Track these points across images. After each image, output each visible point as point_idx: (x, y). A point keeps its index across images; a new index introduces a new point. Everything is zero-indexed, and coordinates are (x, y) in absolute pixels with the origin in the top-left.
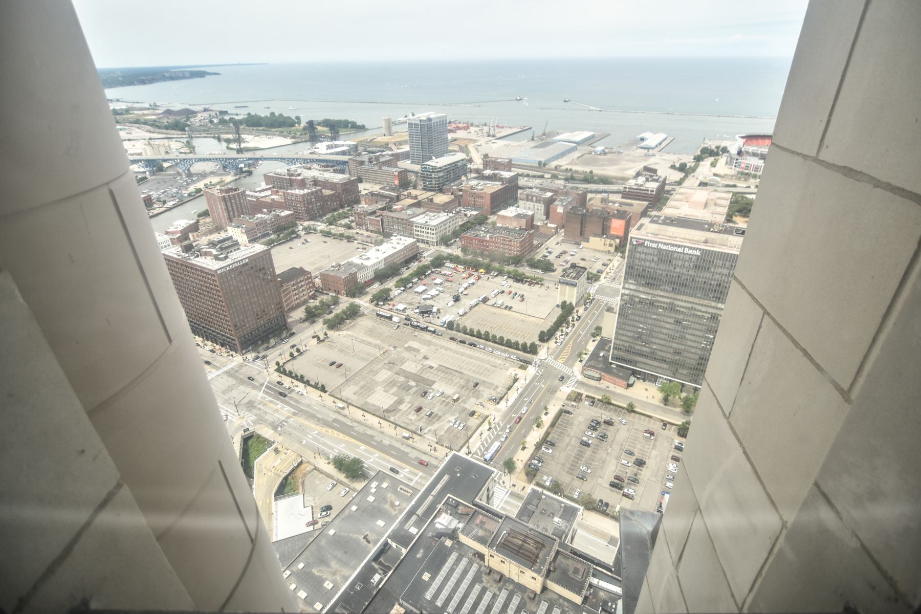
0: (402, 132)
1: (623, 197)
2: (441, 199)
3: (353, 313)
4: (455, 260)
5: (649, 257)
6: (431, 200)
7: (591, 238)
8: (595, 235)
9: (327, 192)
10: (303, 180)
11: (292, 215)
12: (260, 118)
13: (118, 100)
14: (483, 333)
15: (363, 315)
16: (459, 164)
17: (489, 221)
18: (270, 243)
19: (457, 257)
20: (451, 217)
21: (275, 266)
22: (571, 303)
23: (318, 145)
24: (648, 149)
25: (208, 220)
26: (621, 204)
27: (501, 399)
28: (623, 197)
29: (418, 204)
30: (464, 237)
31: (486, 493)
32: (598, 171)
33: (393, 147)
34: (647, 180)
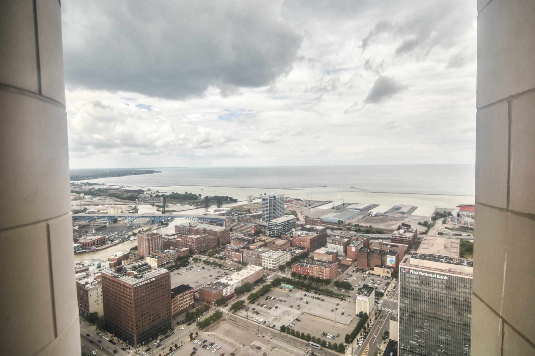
1: (392, 242)
2: (280, 242)
3: (218, 316)
5: (415, 281)
6: (274, 243)
7: (375, 268)
8: (376, 266)
9: (211, 237)
10: (198, 230)
11: (187, 250)
14: (306, 335)
16: (291, 222)
17: (309, 256)
18: (171, 268)
21: (172, 283)
22: (366, 314)
24: (403, 213)
26: (391, 246)
29: (265, 245)
32: (375, 226)
34: (405, 232)
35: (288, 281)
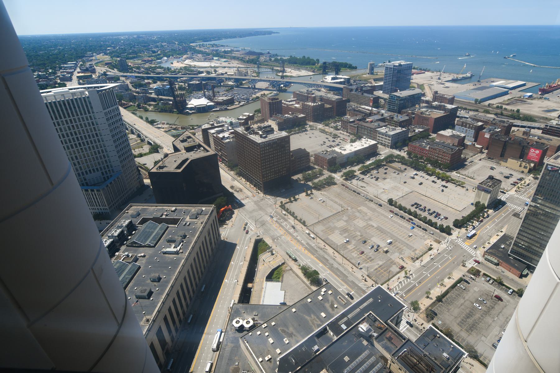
0: (381, 72)
4: (402, 160)
8: (514, 158)
9: (327, 106)
10: (315, 97)
12: (297, 59)
13: (227, 46)
15: (335, 184)
16: (416, 96)
19: (403, 157)
20: (404, 131)
23: (327, 77)
25: (259, 115)
27: (417, 259)
28: (542, 133)
29: (383, 120)
30: (411, 146)
31: (396, 318)
33: (373, 81)
35: (402, 160)
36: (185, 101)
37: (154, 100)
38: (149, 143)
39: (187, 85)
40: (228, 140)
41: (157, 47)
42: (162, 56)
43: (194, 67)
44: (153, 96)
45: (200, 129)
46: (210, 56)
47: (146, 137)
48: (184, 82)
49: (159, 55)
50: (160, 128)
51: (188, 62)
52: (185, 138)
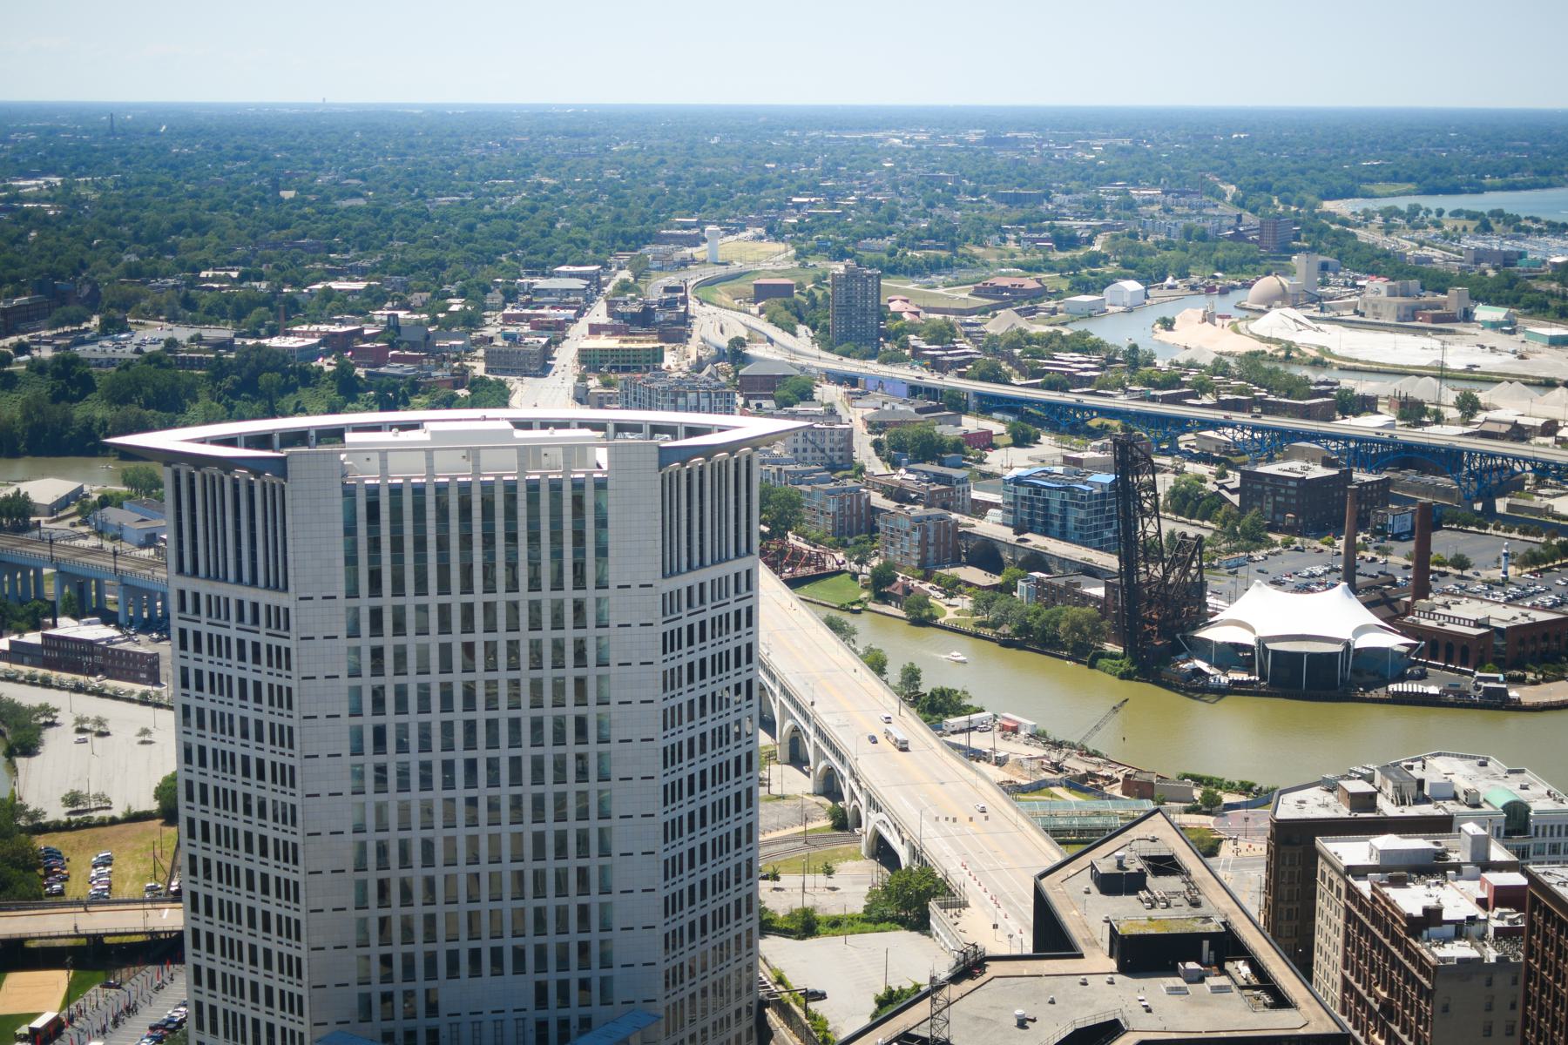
36: (1201, 588)
37: (987, 555)
38: (882, 852)
39: (1234, 479)
40: (1459, 950)
41: (1094, 208)
42: (1109, 269)
43: (1317, 363)
44: (992, 527)
45: (1261, 820)
46: (1452, 299)
47: (873, 804)
48: (1223, 459)
49: (1094, 260)
50: (975, 755)
51: (1282, 324)
52: (1135, 866)
